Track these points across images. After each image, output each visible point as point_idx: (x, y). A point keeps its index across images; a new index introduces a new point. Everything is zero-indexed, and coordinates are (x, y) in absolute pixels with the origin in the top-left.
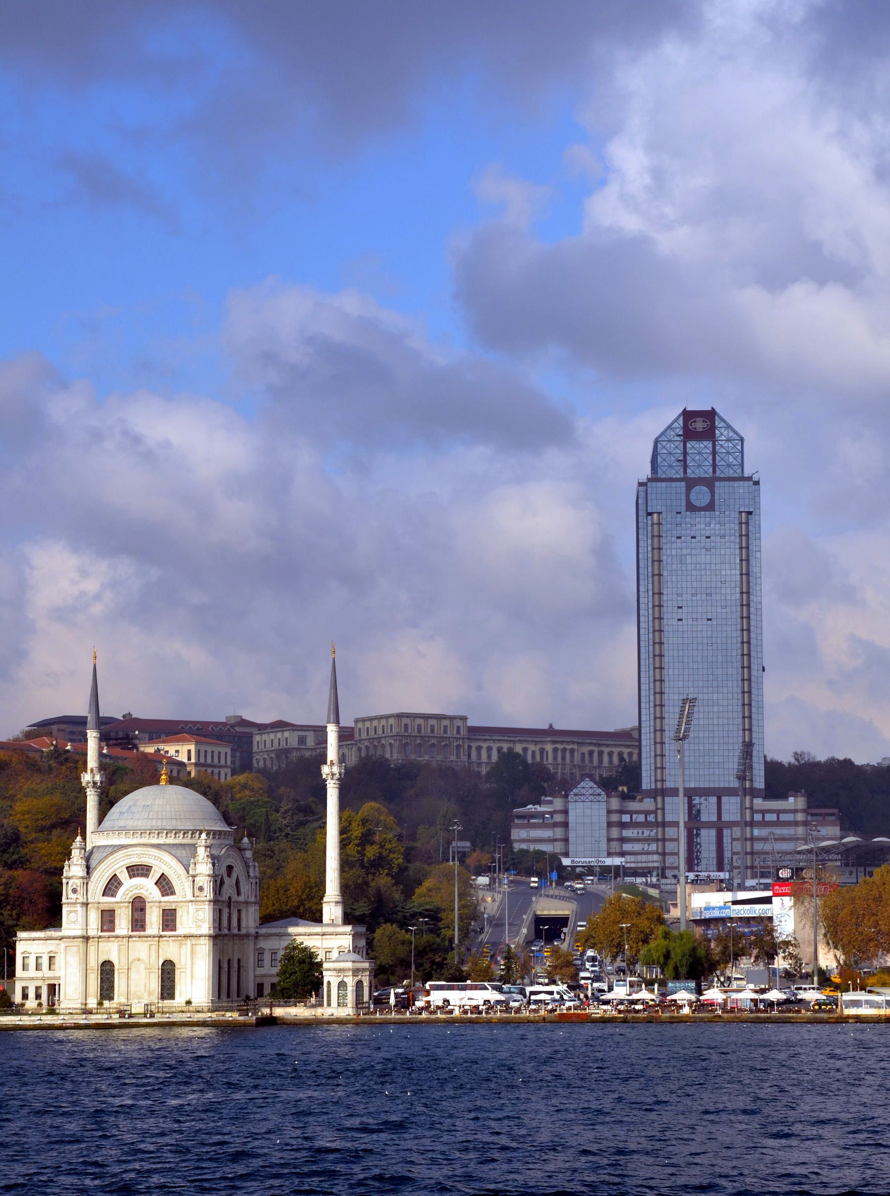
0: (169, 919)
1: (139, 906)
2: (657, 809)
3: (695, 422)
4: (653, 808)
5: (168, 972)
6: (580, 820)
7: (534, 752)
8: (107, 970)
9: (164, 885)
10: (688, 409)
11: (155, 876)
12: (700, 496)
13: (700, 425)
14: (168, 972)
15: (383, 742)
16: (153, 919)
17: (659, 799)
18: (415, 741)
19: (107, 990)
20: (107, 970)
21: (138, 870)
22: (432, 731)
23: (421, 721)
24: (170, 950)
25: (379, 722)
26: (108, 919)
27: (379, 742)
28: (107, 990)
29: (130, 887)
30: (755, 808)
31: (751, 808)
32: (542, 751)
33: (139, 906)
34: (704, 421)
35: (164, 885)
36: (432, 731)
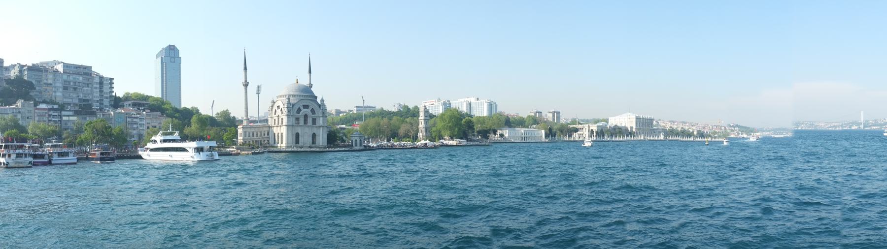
0: (314, 121)
1: (306, 116)
5: (314, 135)
8: (297, 135)
9: (313, 111)
11: (310, 109)
12: (173, 60)
14: (314, 135)
16: (310, 121)
19: (297, 142)
20: (297, 135)
21: (306, 107)
24: (315, 131)
26: (297, 119)
28: (297, 142)
29: (304, 111)
33: (306, 116)
35: (313, 111)
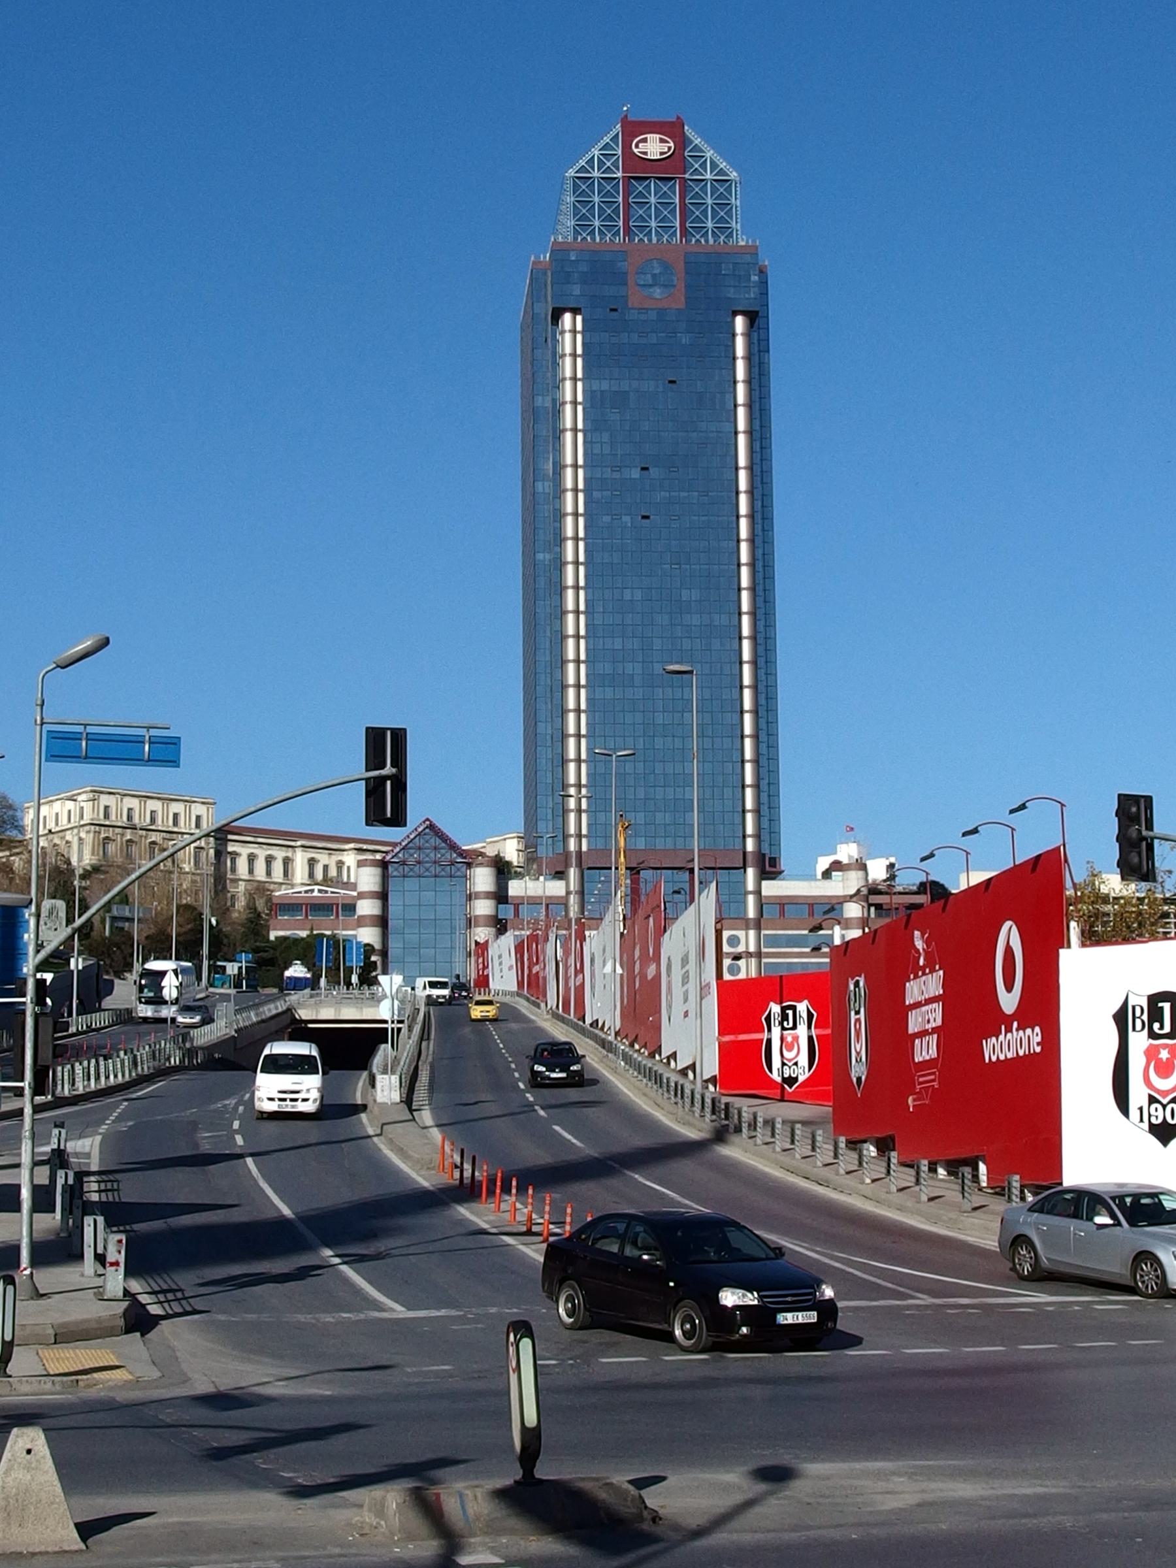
2: (568, 893)
3: (645, 140)
4: (563, 893)
6: (413, 914)
7: (326, 867)
10: (630, 119)
13: (653, 147)
15: (68, 838)
17: (573, 872)
18: (123, 835)
22: (153, 821)
23: (134, 803)
25: (63, 806)
27: (63, 838)
30: (764, 893)
31: (758, 892)
32: (340, 864)
34: (662, 141)
36: (153, 821)
